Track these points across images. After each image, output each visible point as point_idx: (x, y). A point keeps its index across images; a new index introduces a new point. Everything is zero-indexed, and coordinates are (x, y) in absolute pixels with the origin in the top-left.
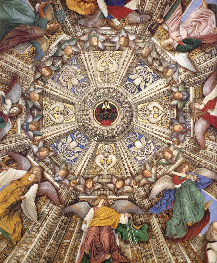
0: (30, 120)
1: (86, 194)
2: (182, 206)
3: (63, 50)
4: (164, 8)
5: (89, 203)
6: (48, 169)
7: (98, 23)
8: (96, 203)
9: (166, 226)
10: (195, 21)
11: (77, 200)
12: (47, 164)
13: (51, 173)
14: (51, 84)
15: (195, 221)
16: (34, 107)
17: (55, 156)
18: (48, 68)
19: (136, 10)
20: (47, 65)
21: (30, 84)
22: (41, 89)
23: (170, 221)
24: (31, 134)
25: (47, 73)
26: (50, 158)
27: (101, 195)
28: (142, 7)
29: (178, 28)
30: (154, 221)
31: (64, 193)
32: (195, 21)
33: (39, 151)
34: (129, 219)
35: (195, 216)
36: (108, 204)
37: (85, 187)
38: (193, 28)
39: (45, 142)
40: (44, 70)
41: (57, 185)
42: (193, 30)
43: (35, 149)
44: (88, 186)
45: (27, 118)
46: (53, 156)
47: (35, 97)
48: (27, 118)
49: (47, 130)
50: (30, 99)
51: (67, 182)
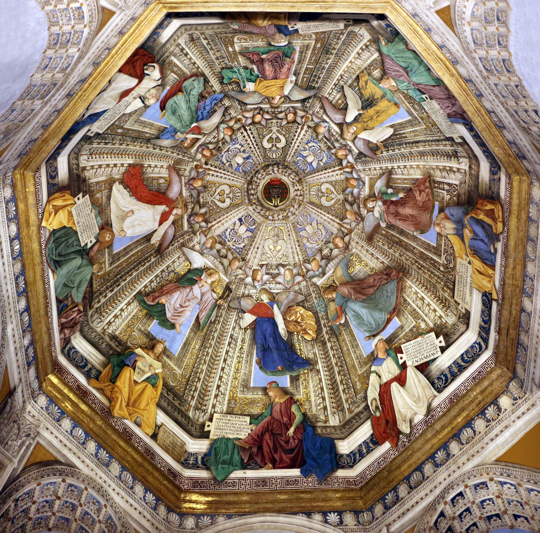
0: (356, 191)
1: (293, 108)
2: (189, 108)
3: (320, 266)
4: (217, 317)
5: (290, 99)
6: (337, 136)
7: (284, 297)
8: (283, 99)
9: (204, 85)
10: (186, 307)
11: (303, 101)
12: (337, 140)
13: (332, 131)
14: (334, 228)
15: (175, 98)
16: (351, 204)
17: (329, 148)
18: (337, 247)
19: (244, 312)
20: (337, 250)
21: (355, 230)
22: (344, 223)
23: (200, 91)
24: (355, 176)
25: (338, 240)
26: (335, 147)
27: (277, 107)
28: (239, 316)
29: (202, 296)
30: (217, 86)
31: (317, 108)
32: (186, 307)
33: (346, 155)
34: (245, 87)
35: (175, 103)
36: (269, 100)
37: (295, 114)
38: (188, 298)
39: (341, 164)
40: (341, 245)
41: (325, 117)
42: (187, 296)
43: (350, 158)
44: (292, 115)
45: (359, 194)
46: (331, 149)
47: (350, 215)
48: (359, 194)
49: (338, 178)
50: (356, 213)
51: (316, 120)
